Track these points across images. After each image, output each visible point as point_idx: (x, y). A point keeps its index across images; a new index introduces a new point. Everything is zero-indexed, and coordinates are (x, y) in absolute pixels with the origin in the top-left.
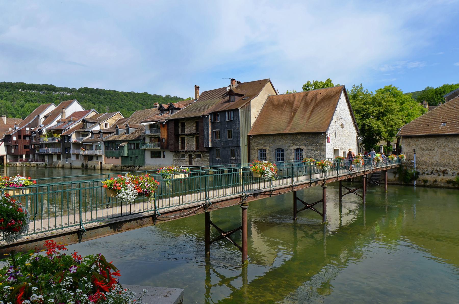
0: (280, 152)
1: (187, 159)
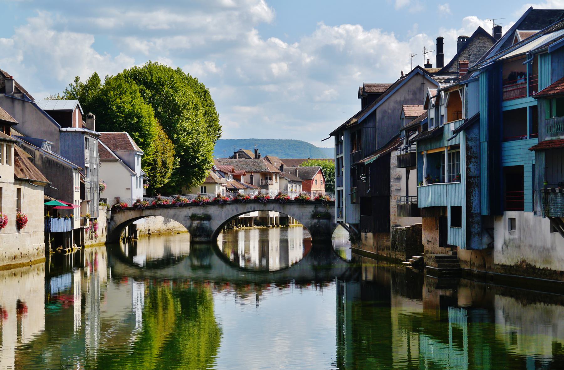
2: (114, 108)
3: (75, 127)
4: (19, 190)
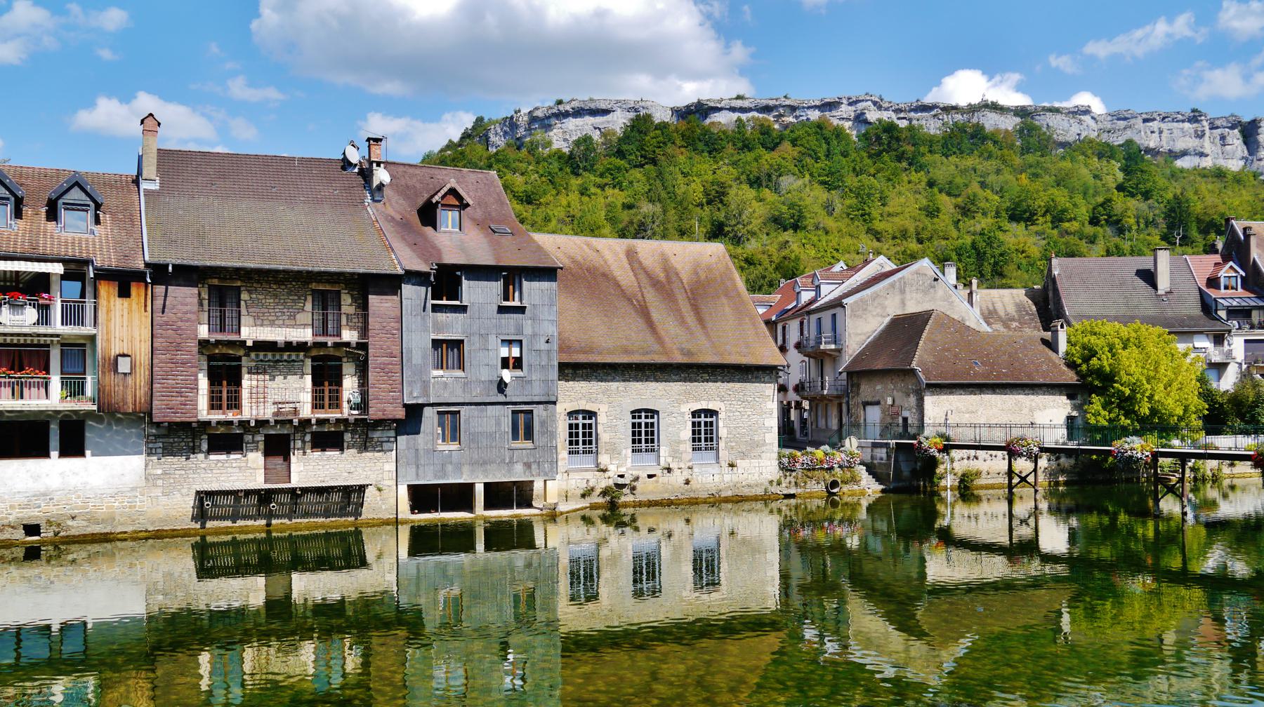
0: (643, 420)
1: (256, 458)
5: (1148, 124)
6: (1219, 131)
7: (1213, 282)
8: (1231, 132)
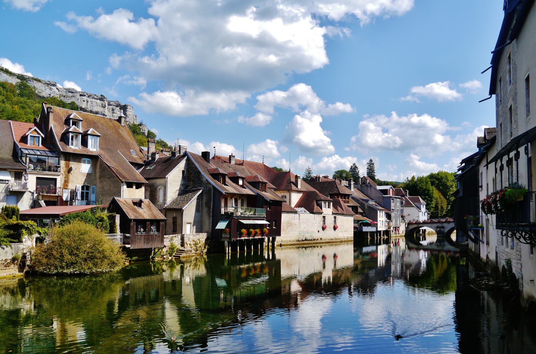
2: (418, 188)
3: (390, 195)
4: (335, 217)
5: (82, 97)
6: (112, 107)
7: (24, 139)
8: (116, 108)
